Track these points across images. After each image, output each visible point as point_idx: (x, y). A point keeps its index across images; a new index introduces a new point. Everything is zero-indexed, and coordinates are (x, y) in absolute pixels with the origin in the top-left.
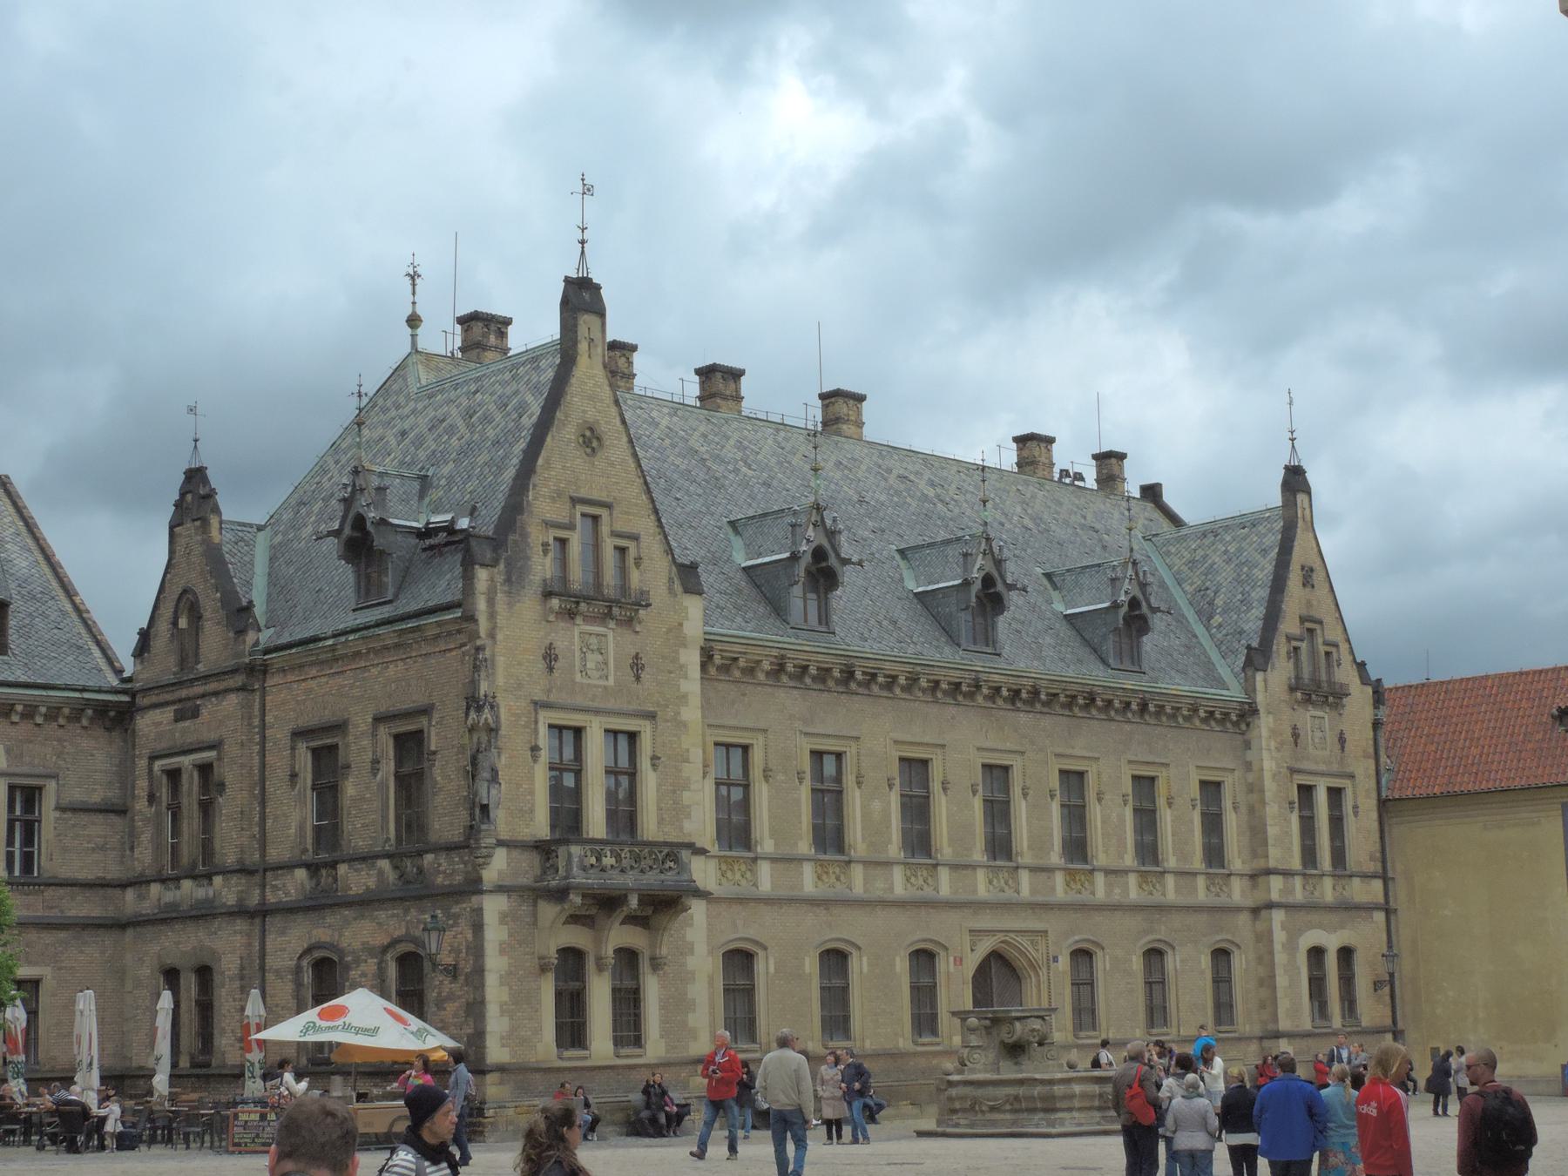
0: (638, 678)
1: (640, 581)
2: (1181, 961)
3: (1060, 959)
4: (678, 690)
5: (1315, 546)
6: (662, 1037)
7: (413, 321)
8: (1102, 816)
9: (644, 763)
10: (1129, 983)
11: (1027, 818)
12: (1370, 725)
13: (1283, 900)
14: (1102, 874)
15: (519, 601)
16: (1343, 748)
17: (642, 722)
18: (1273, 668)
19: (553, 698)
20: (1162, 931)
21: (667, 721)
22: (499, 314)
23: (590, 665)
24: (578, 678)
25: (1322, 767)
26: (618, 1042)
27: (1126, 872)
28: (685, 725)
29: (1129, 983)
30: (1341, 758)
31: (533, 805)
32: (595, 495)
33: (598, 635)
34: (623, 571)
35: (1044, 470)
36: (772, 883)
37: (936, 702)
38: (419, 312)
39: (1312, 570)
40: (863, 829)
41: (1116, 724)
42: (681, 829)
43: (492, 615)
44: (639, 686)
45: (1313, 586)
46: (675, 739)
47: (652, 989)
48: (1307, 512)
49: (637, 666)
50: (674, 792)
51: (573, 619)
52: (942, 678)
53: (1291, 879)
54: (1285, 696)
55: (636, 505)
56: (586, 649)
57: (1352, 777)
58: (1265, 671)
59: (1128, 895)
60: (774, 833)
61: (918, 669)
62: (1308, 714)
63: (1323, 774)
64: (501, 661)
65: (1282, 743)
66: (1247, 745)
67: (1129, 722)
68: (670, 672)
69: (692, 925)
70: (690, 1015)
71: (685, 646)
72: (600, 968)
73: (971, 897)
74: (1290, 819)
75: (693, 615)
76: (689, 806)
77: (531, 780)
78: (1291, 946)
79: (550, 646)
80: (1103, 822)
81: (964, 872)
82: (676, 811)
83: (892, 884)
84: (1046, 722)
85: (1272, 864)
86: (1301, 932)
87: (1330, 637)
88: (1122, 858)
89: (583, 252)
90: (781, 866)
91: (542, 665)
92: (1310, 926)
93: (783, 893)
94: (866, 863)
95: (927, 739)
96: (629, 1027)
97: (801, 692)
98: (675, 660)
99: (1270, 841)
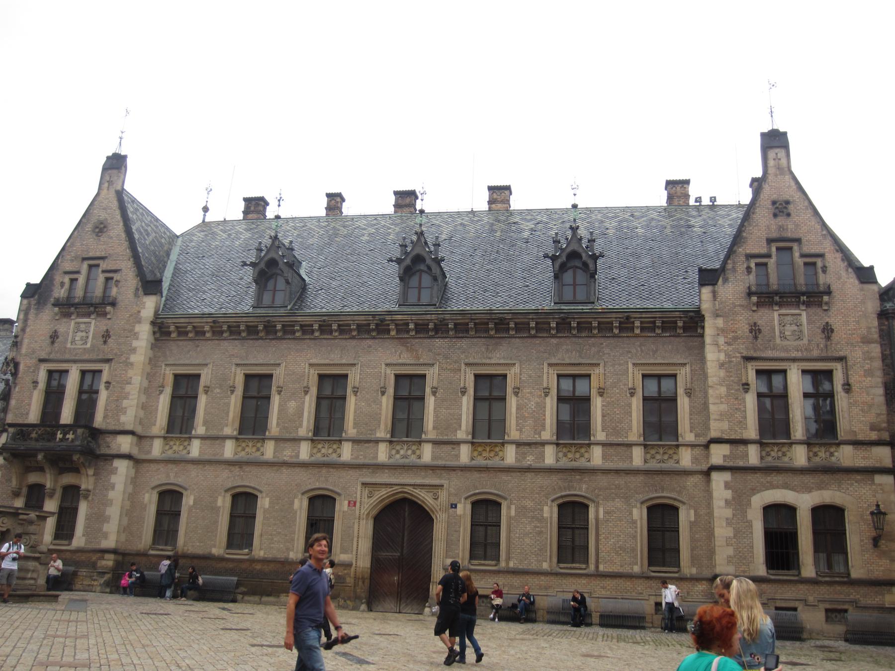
0: (105, 342)
1: (117, 293)
2: (605, 513)
3: (459, 506)
4: (131, 346)
5: (793, 183)
6: (83, 535)
7: (206, 209)
8: (517, 405)
9: (102, 387)
10: (536, 527)
11: (435, 409)
12: (875, 316)
13: (726, 464)
14: (514, 447)
15: (42, 312)
16: (828, 338)
17: (104, 365)
18: (726, 280)
19: (52, 357)
20: (581, 489)
21: (121, 363)
22: (256, 196)
23: (77, 339)
24: (69, 345)
25: (799, 355)
26: (57, 536)
27: (543, 444)
28: (132, 364)
29: (536, 527)
30: (826, 346)
31: (29, 411)
32: (98, 254)
33: (85, 323)
34: (106, 288)
35: (678, 201)
36: (200, 452)
37: (353, 338)
38: (208, 206)
39: (787, 202)
40: (278, 418)
41: (540, 340)
42: (118, 420)
43: (26, 320)
44: (106, 346)
45: (789, 215)
46: (124, 372)
47: (83, 508)
48: (784, 162)
49: (106, 336)
50: (117, 400)
51: (71, 316)
52: (371, 322)
53: (742, 448)
54: (744, 302)
55: (122, 255)
56: (77, 330)
57: (841, 359)
58: (714, 283)
59: (544, 461)
60: (205, 423)
61: (325, 318)
62: (776, 314)
63: (794, 360)
64: (26, 341)
65: (735, 338)
66: (702, 345)
67: (553, 336)
68: (127, 337)
69: (116, 474)
70: (105, 525)
71: (139, 322)
72: (51, 496)
73: (374, 462)
74: (744, 399)
75: (149, 305)
76: (125, 408)
77: (31, 398)
78: (739, 502)
79: (56, 331)
80: (517, 409)
81: (367, 445)
82: (117, 409)
83: (299, 452)
84: (464, 343)
85: (714, 434)
86: (754, 491)
87: (814, 250)
88: (540, 434)
89: (120, 143)
90: (208, 442)
91: (49, 341)
92: (772, 486)
93: (206, 457)
94: (277, 440)
95: (344, 361)
96: (65, 529)
97: (239, 341)
98: (131, 331)
99: (712, 417)
